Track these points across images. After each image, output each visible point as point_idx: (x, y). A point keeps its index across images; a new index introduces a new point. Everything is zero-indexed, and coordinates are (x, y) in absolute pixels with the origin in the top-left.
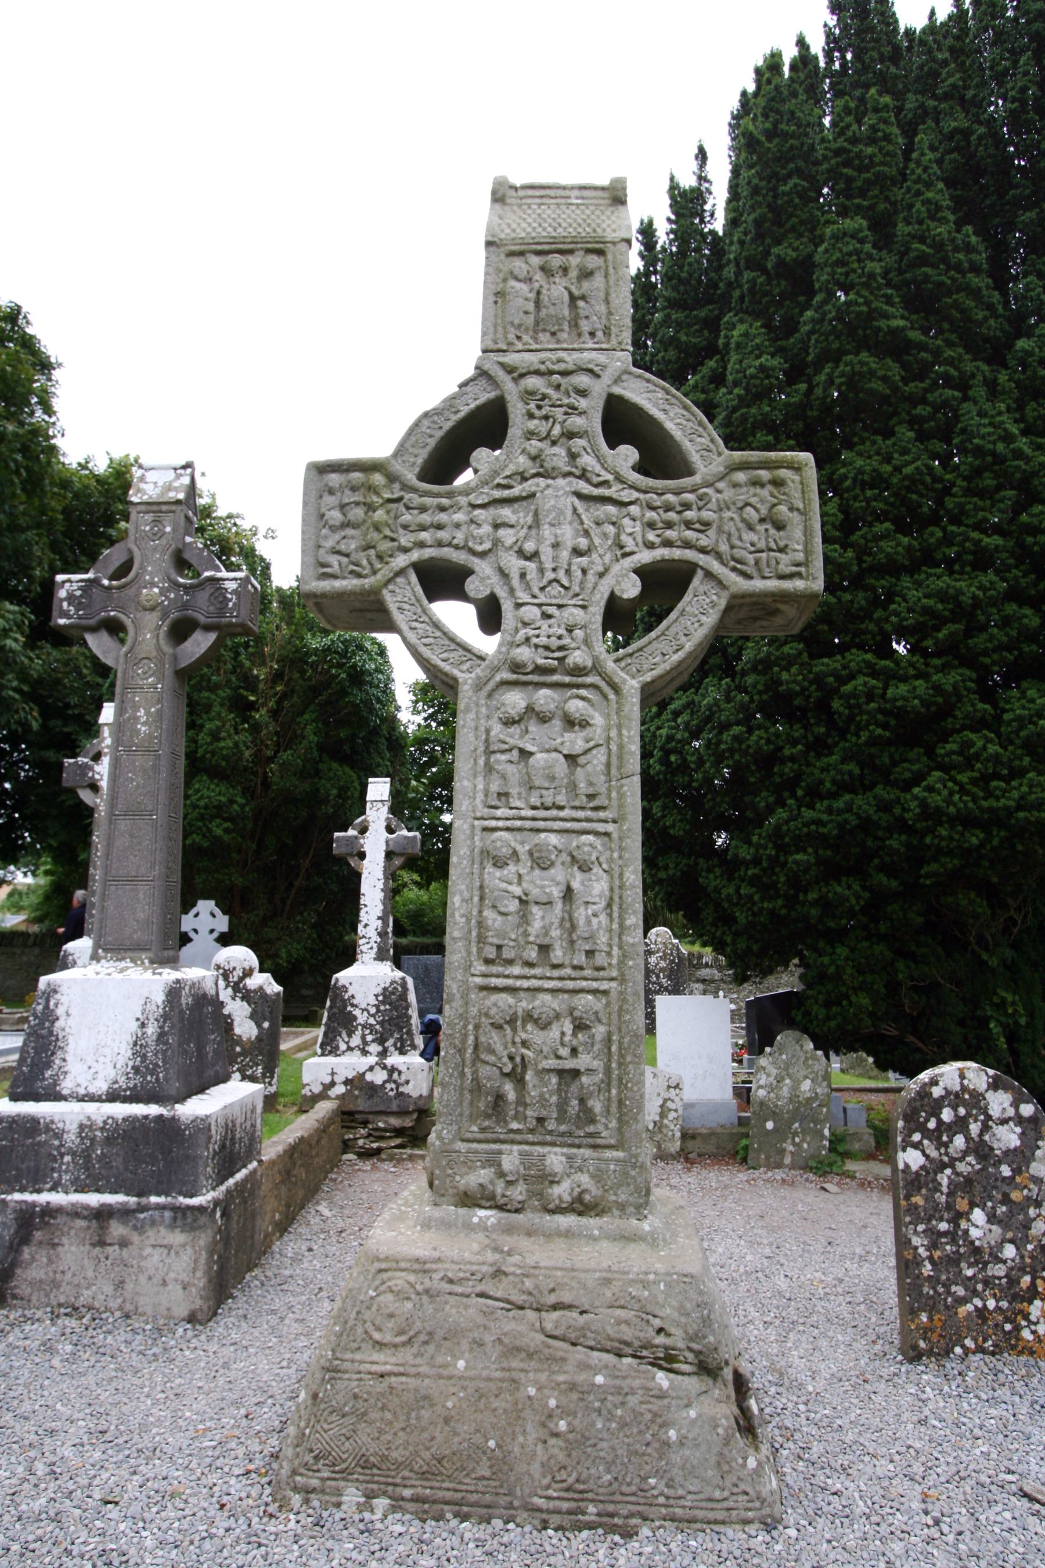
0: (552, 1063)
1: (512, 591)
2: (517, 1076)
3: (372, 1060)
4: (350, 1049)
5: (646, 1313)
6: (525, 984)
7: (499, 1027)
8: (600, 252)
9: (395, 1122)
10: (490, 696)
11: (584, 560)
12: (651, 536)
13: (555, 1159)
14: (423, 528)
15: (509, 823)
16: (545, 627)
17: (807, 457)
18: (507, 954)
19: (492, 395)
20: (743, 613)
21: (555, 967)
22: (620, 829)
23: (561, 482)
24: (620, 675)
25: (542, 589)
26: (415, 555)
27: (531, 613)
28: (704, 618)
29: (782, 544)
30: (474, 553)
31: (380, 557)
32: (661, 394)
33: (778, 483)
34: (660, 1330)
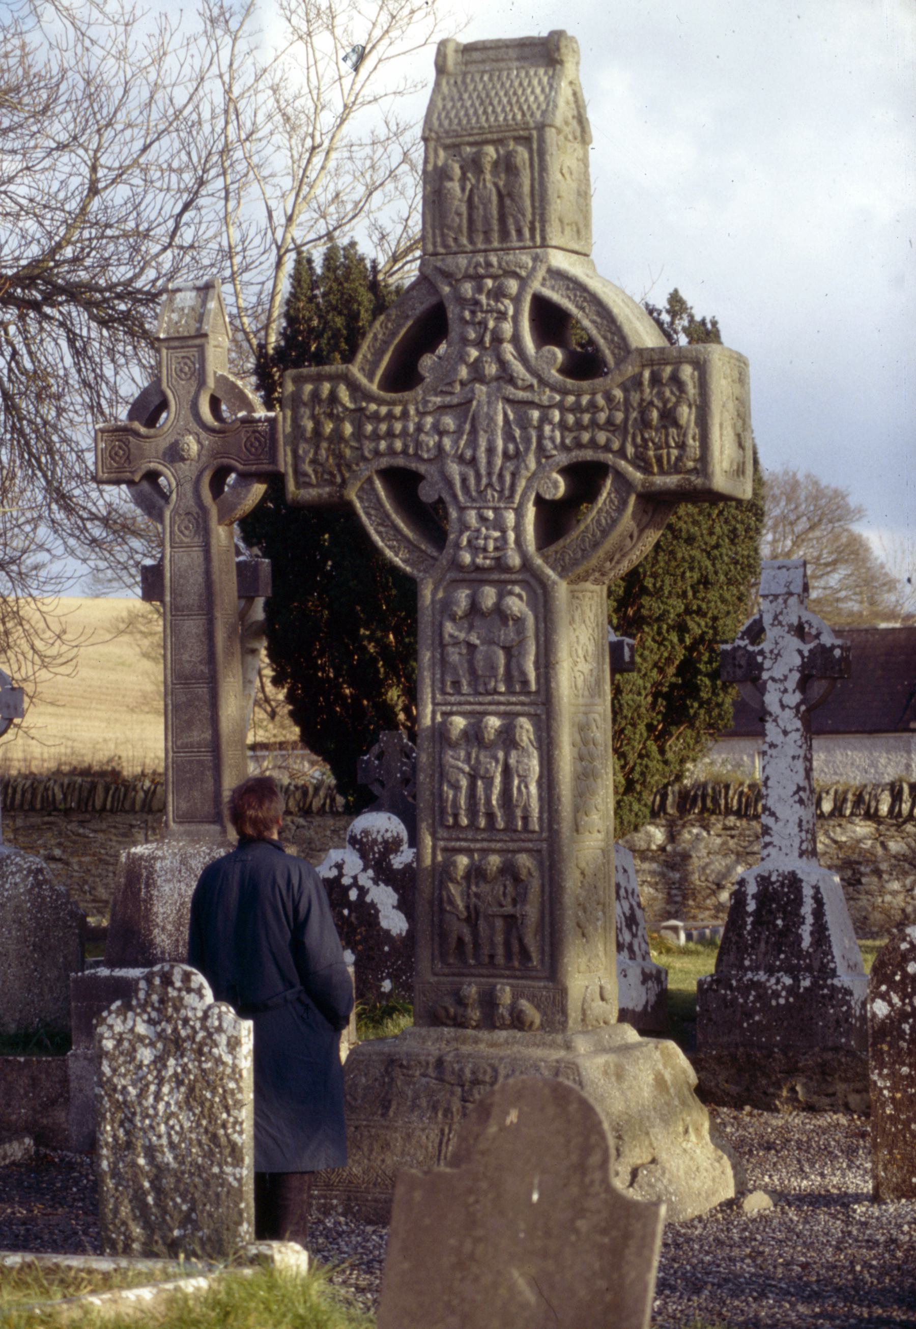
1: (455, 496)
11: (510, 466)
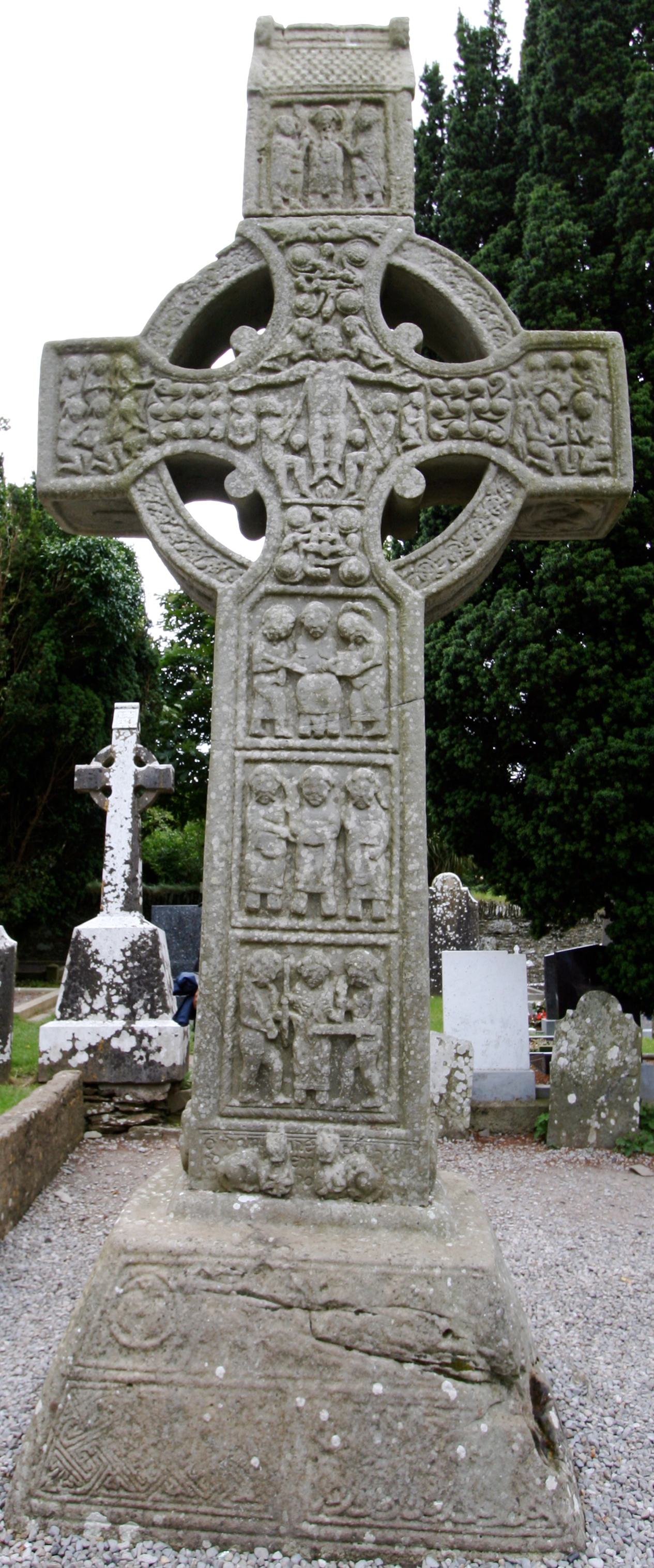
0: (323, 1028)
1: (278, 489)
2: (284, 1044)
3: (119, 1024)
4: (93, 1011)
5: (431, 1312)
6: (294, 937)
7: (264, 987)
8: (379, 103)
9: (145, 1095)
10: (253, 609)
11: (360, 455)
12: (437, 427)
13: (327, 1137)
14: (177, 418)
15: (274, 754)
16: (316, 530)
17: (614, 336)
18: (272, 903)
19: (255, 266)
20: (541, 515)
21: (327, 918)
22: (401, 761)
23: (333, 365)
24: (401, 585)
25: (313, 487)
26: (168, 449)
27: (300, 514)
28: (497, 521)
29: (585, 436)
30: (235, 446)
31: (128, 451)
32: (448, 265)
33: (581, 366)
34: (447, 1332)
